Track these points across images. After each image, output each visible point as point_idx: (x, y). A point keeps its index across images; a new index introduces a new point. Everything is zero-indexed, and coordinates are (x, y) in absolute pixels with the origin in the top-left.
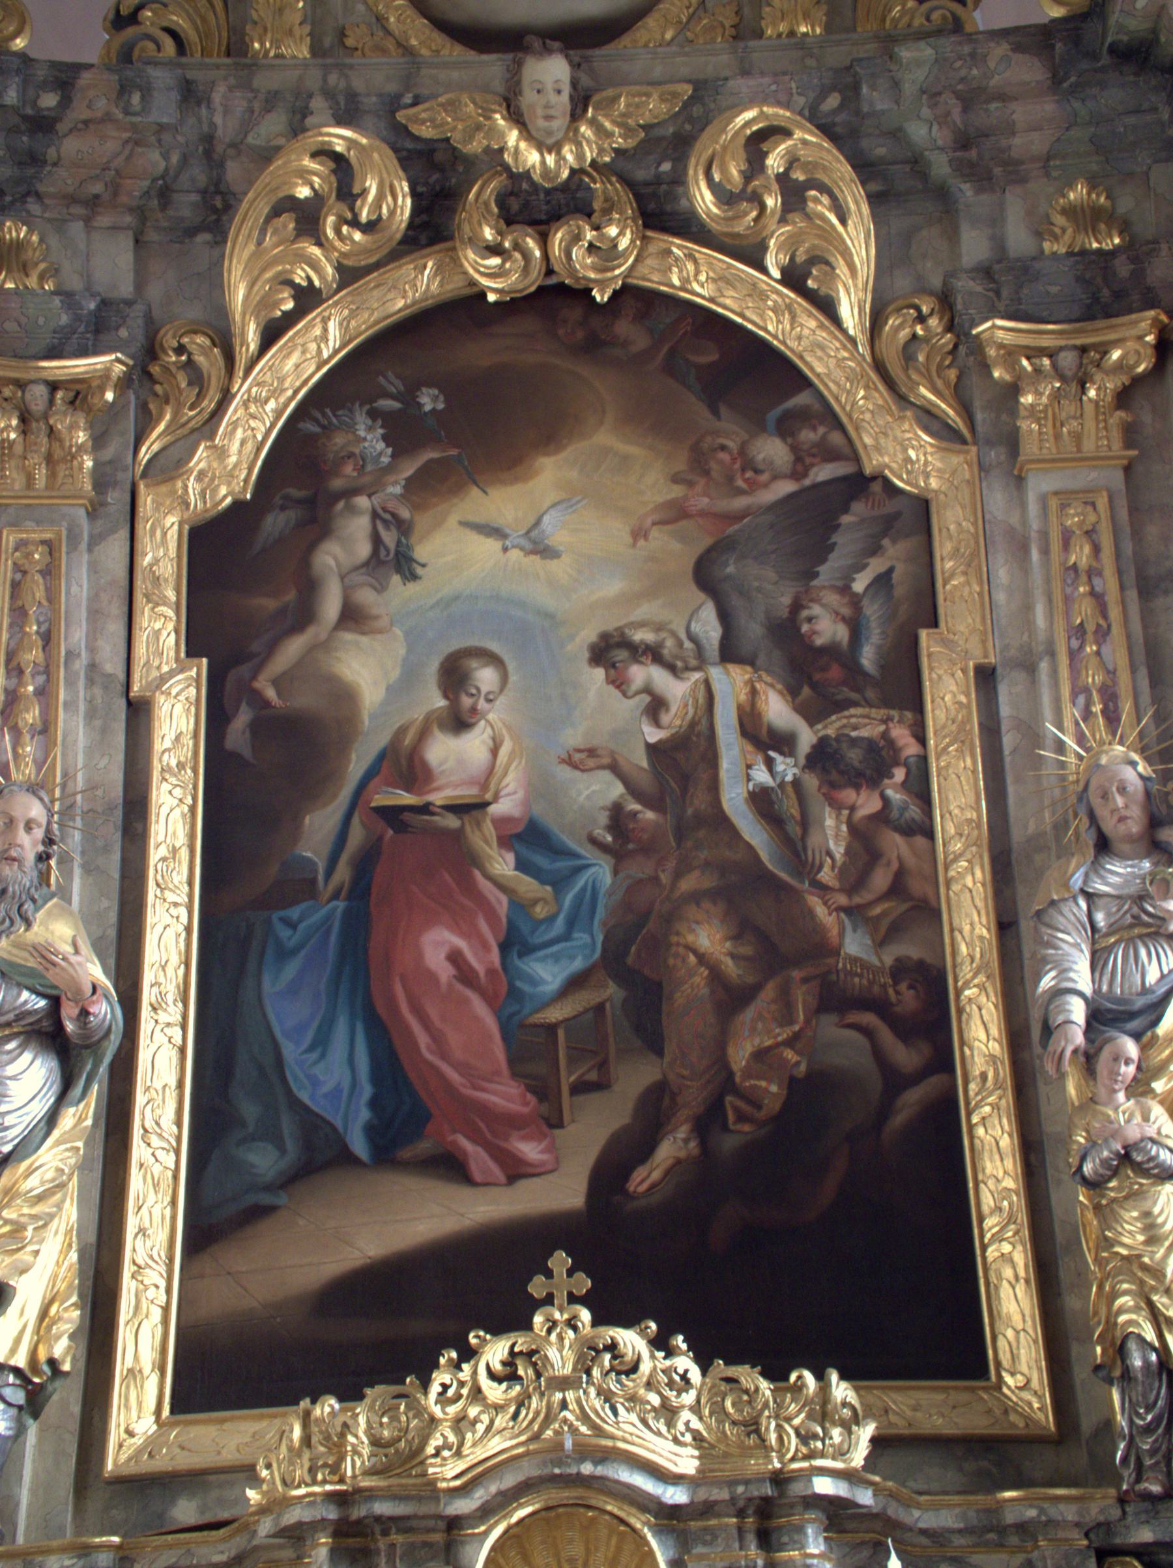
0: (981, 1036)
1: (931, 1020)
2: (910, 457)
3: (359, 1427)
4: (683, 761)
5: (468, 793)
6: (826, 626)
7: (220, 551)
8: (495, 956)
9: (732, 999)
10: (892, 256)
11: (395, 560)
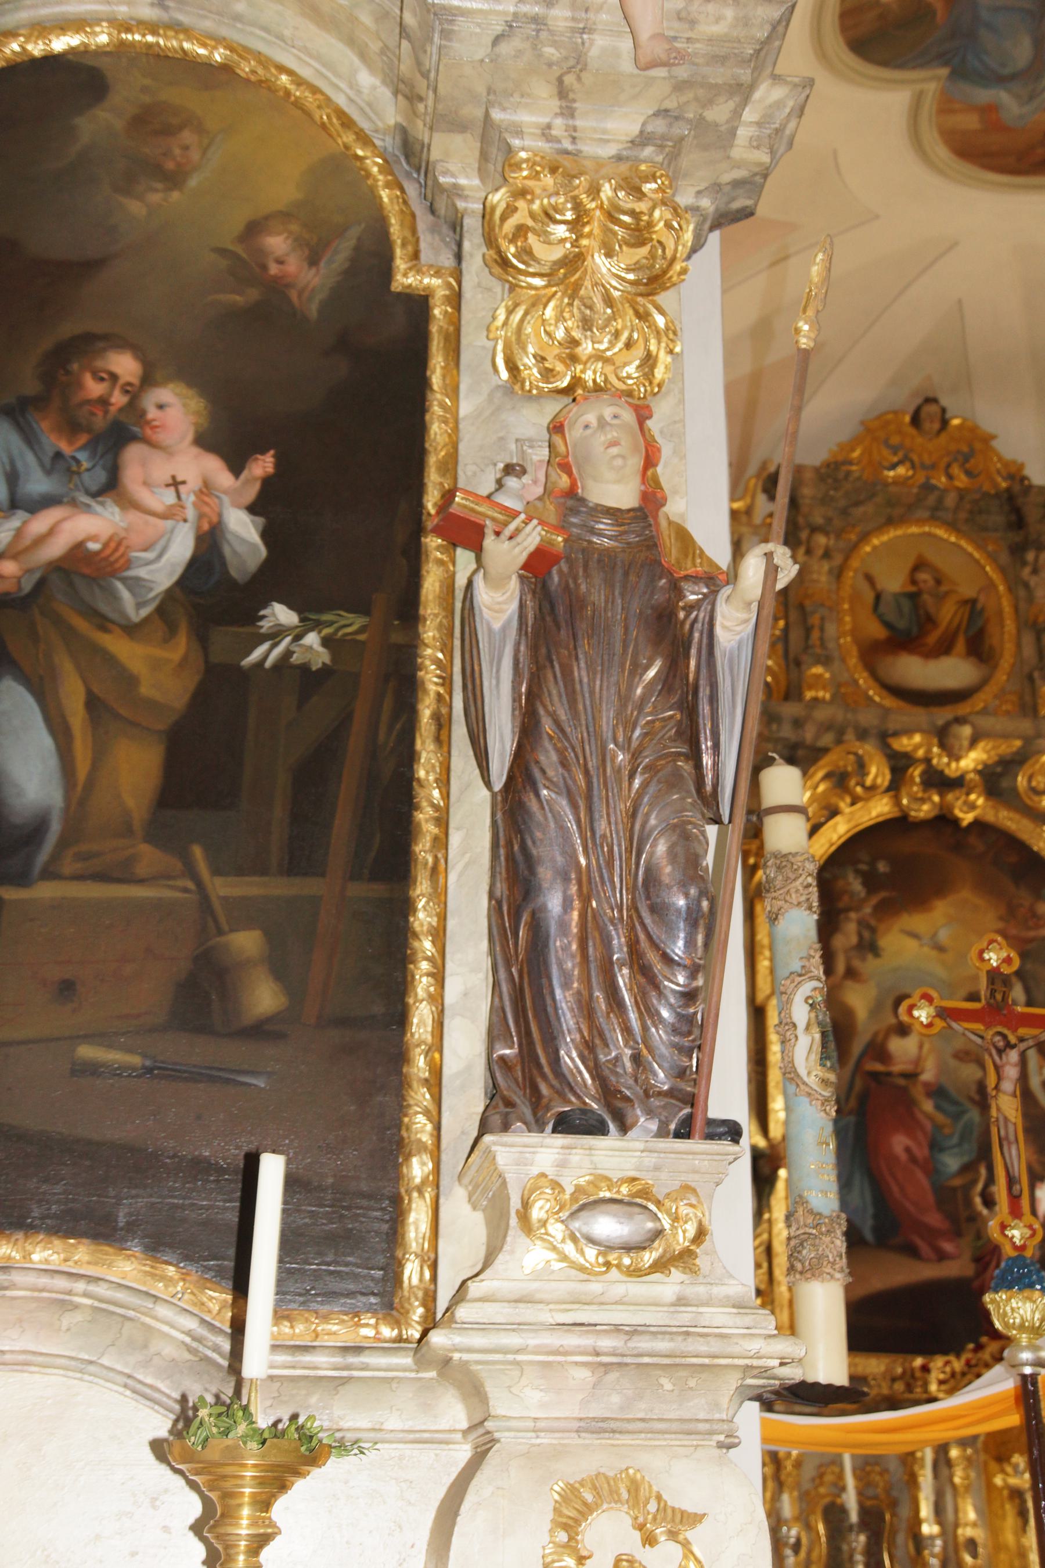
5: (908, 1068)
8: (926, 1152)
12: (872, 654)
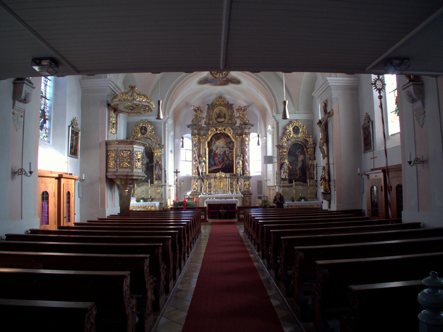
0: (235, 162)
1: (233, 162)
2: (234, 140)
3: (214, 174)
4: (225, 152)
6: (230, 147)
7: (208, 143)
9: (226, 161)
10: (233, 132)
11: (215, 144)
12: (216, 119)
